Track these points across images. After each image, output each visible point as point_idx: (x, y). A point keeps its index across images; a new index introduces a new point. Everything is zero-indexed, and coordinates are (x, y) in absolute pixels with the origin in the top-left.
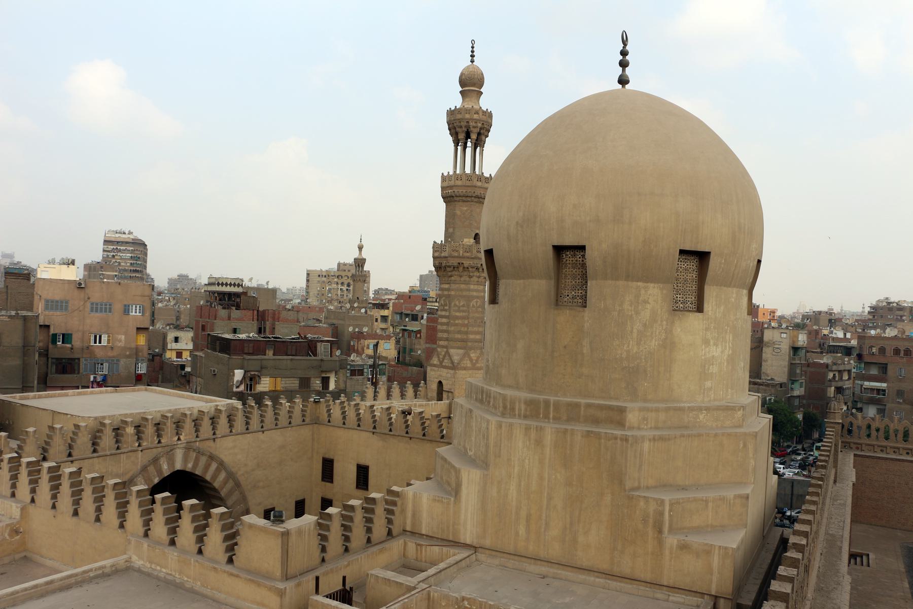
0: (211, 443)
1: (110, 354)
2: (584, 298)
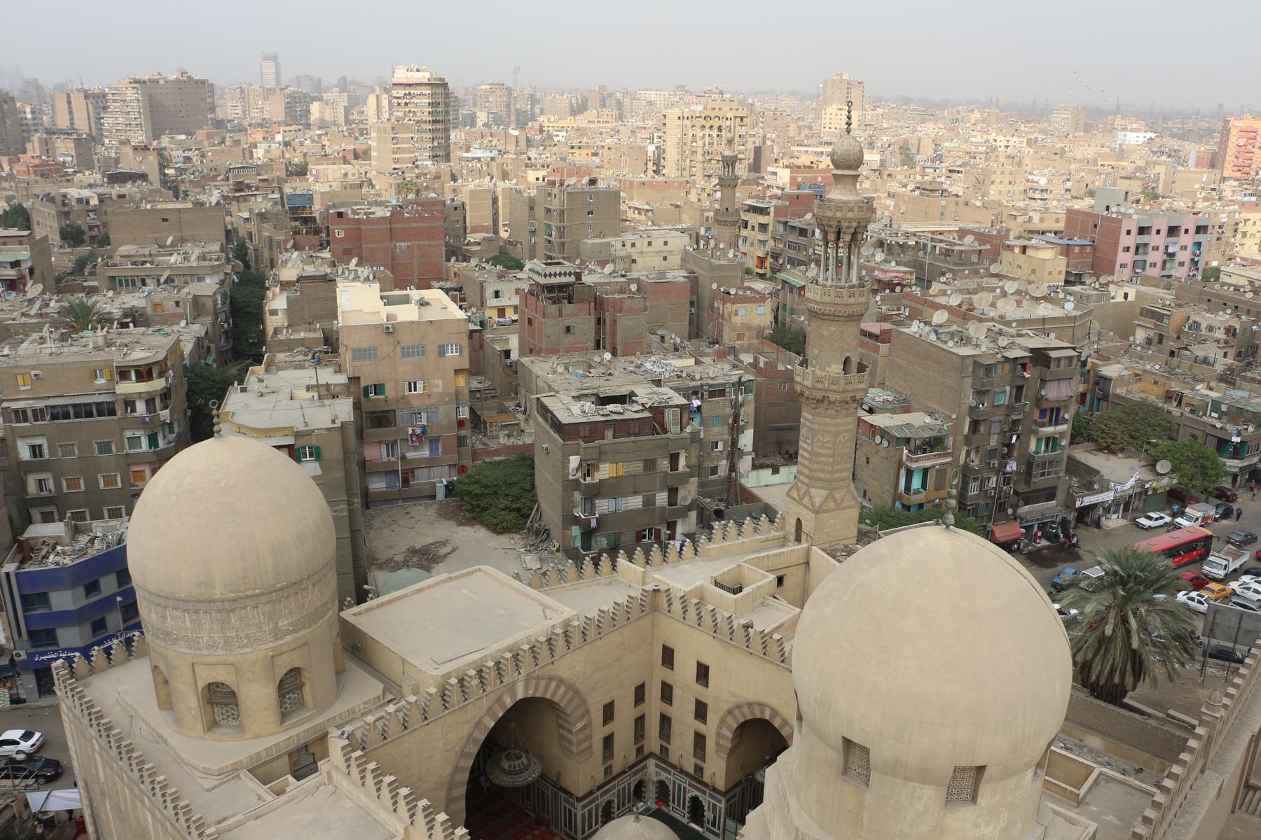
0: (551, 667)
1: (427, 402)
2: (868, 777)
